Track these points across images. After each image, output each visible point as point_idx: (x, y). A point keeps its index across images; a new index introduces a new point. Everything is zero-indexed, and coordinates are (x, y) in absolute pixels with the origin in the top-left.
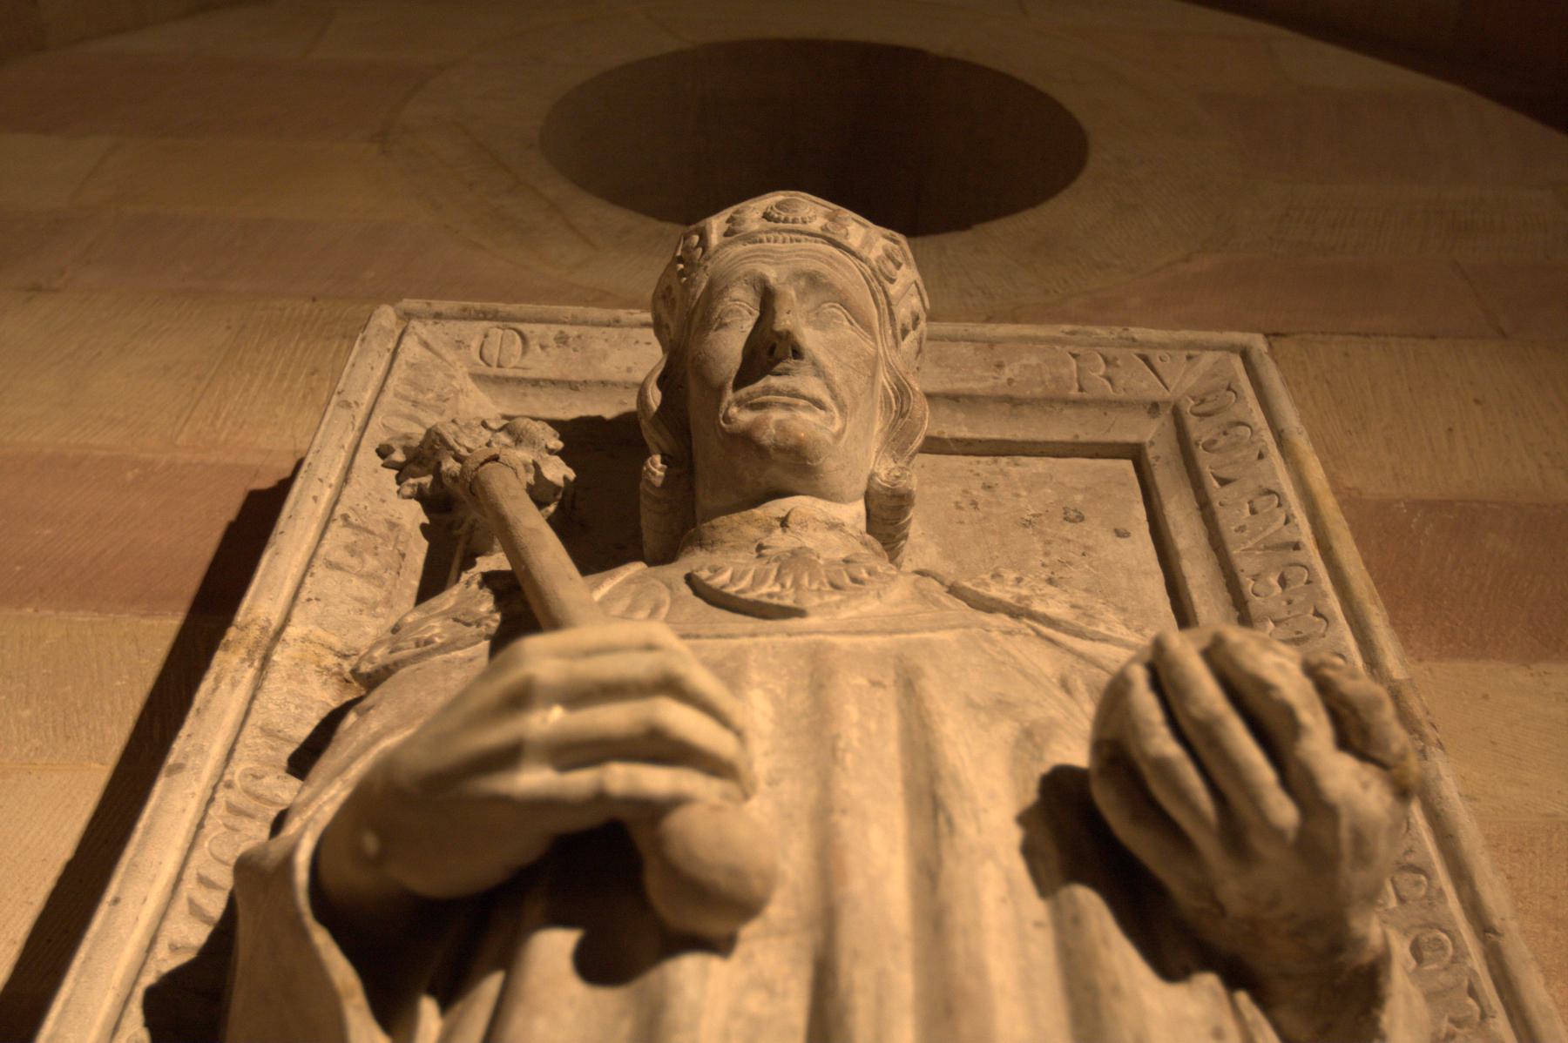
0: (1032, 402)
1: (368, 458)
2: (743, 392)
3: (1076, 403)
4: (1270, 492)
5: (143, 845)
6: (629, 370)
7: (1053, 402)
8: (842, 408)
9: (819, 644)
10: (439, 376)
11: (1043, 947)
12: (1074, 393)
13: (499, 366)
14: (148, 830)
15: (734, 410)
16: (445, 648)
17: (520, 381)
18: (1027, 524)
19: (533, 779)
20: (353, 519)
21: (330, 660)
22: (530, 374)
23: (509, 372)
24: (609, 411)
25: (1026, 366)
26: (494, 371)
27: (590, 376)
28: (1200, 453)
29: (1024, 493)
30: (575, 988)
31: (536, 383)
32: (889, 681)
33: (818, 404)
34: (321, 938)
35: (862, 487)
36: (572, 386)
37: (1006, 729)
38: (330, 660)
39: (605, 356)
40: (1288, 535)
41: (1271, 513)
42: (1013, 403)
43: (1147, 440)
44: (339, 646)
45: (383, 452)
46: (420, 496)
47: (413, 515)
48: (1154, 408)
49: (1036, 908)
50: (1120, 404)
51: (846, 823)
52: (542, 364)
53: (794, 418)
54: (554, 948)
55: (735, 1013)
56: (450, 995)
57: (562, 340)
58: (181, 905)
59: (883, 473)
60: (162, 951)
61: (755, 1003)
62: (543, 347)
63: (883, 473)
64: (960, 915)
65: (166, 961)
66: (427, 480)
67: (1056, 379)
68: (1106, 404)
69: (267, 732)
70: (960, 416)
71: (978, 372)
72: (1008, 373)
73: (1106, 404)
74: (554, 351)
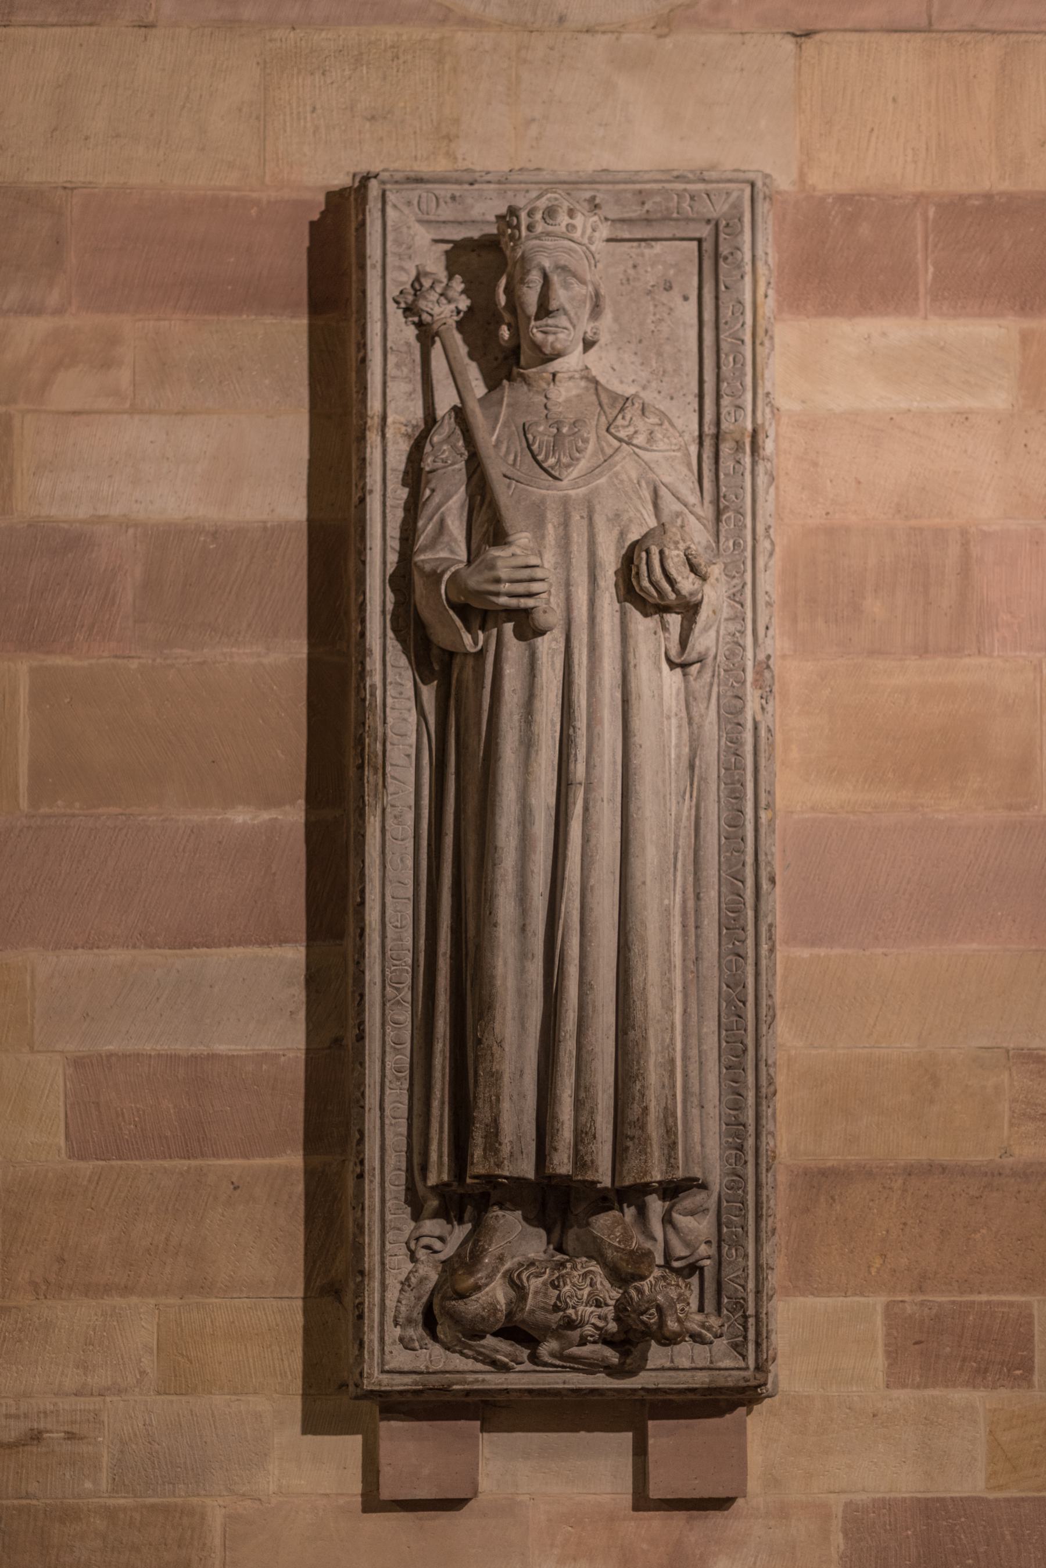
0: (656, 220)
1: (391, 306)
2: (539, 323)
3: (677, 220)
4: (740, 303)
5: (371, 526)
6: (484, 214)
7: (666, 219)
8: (574, 327)
9: (566, 496)
10: (405, 230)
11: (618, 615)
12: (675, 215)
13: (428, 214)
14: (371, 518)
15: (535, 330)
16: (451, 465)
17: (437, 222)
18: (649, 293)
19: (503, 600)
20: (394, 348)
21: (403, 429)
22: (442, 218)
23: (432, 217)
24: (475, 234)
25: (654, 203)
26: (426, 217)
27: (467, 218)
28: (721, 263)
29: (649, 269)
30: (515, 641)
31: (444, 222)
32: (585, 515)
33: (565, 328)
34: (451, 612)
35: (581, 336)
36: (460, 223)
37: (616, 532)
38: (403, 429)
39: (472, 207)
40: (740, 335)
41: (738, 317)
42: (648, 221)
43: (704, 236)
44: (405, 422)
45: (397, 302)
46: (414, 323)
47: (411, 332)
48: (708, 221)
49: (617, 606)
50: (693, 220)
51: (573, 589)
52: (446, 212)
53: (557, 339)
54: (509, 627)
55: (549, 648)
56: (483, 628)
57: (453, 198)
58: (389, 549)
59: (589, 330)
60: (388, 566)
61: (554, 645)
62: (446, 203)
63: (589, 330)
64: (598, 620)
65: (390, 570)
66: (416, 319)
67: (667, 209)
68: (688, 220)
69: (394, 470)
70: (625, 227)
71: (634, 207)
72: (647, 207)
73: (688, 220)
74: (451, 205)
